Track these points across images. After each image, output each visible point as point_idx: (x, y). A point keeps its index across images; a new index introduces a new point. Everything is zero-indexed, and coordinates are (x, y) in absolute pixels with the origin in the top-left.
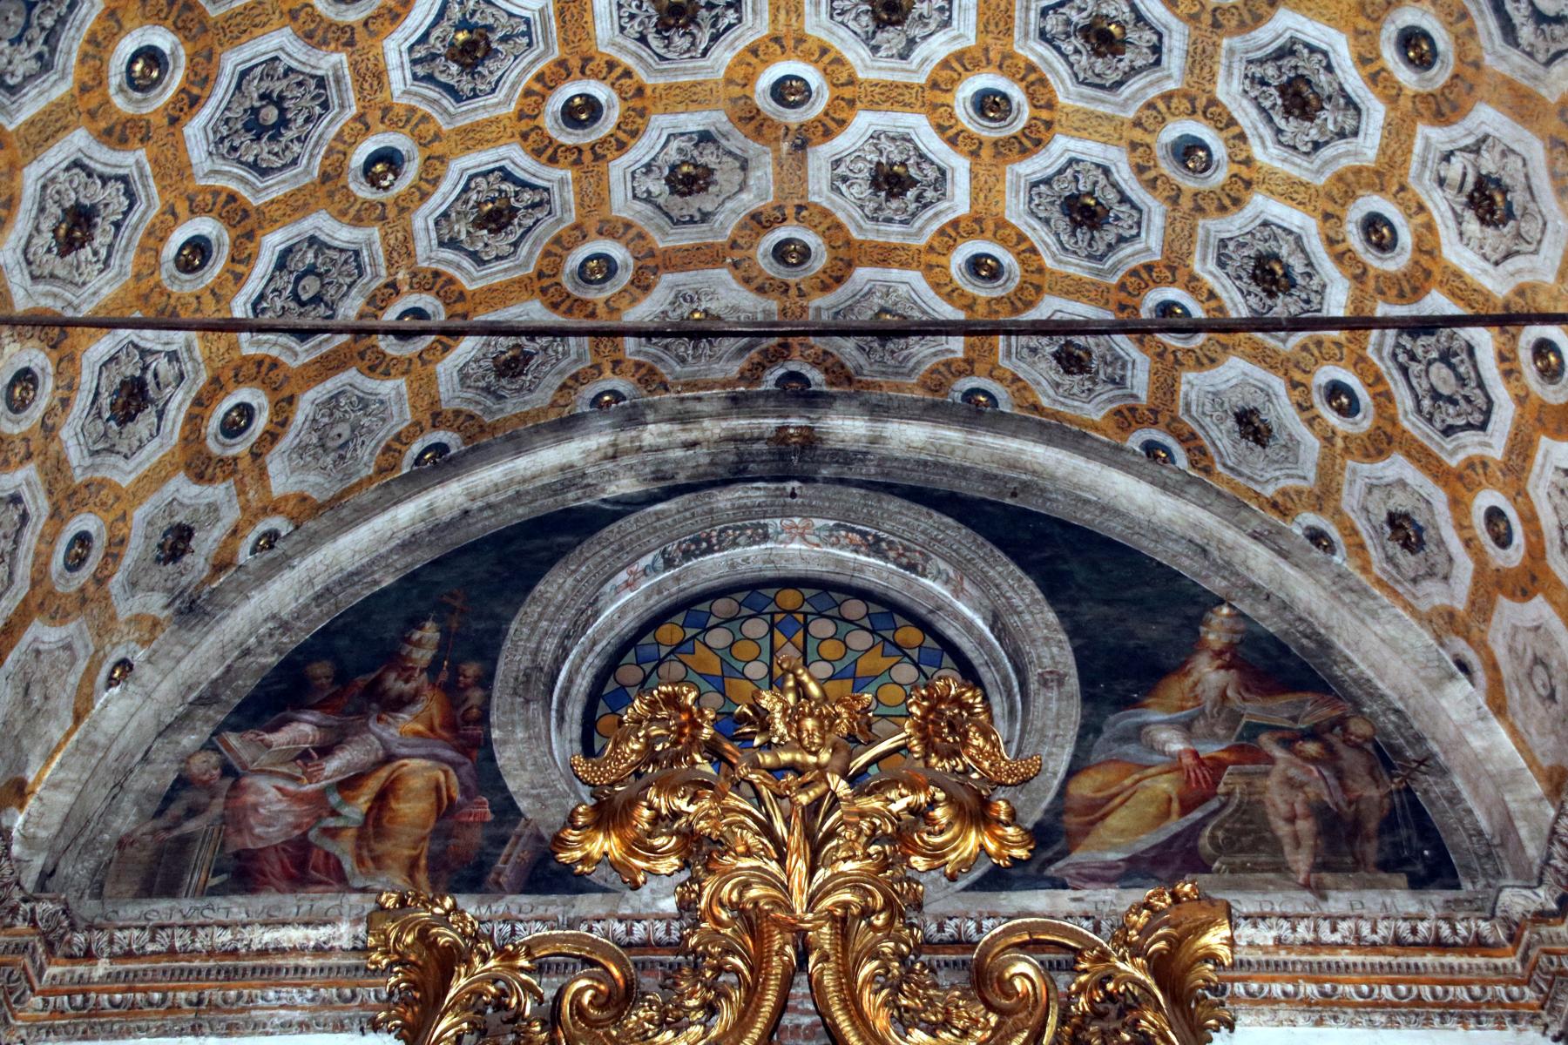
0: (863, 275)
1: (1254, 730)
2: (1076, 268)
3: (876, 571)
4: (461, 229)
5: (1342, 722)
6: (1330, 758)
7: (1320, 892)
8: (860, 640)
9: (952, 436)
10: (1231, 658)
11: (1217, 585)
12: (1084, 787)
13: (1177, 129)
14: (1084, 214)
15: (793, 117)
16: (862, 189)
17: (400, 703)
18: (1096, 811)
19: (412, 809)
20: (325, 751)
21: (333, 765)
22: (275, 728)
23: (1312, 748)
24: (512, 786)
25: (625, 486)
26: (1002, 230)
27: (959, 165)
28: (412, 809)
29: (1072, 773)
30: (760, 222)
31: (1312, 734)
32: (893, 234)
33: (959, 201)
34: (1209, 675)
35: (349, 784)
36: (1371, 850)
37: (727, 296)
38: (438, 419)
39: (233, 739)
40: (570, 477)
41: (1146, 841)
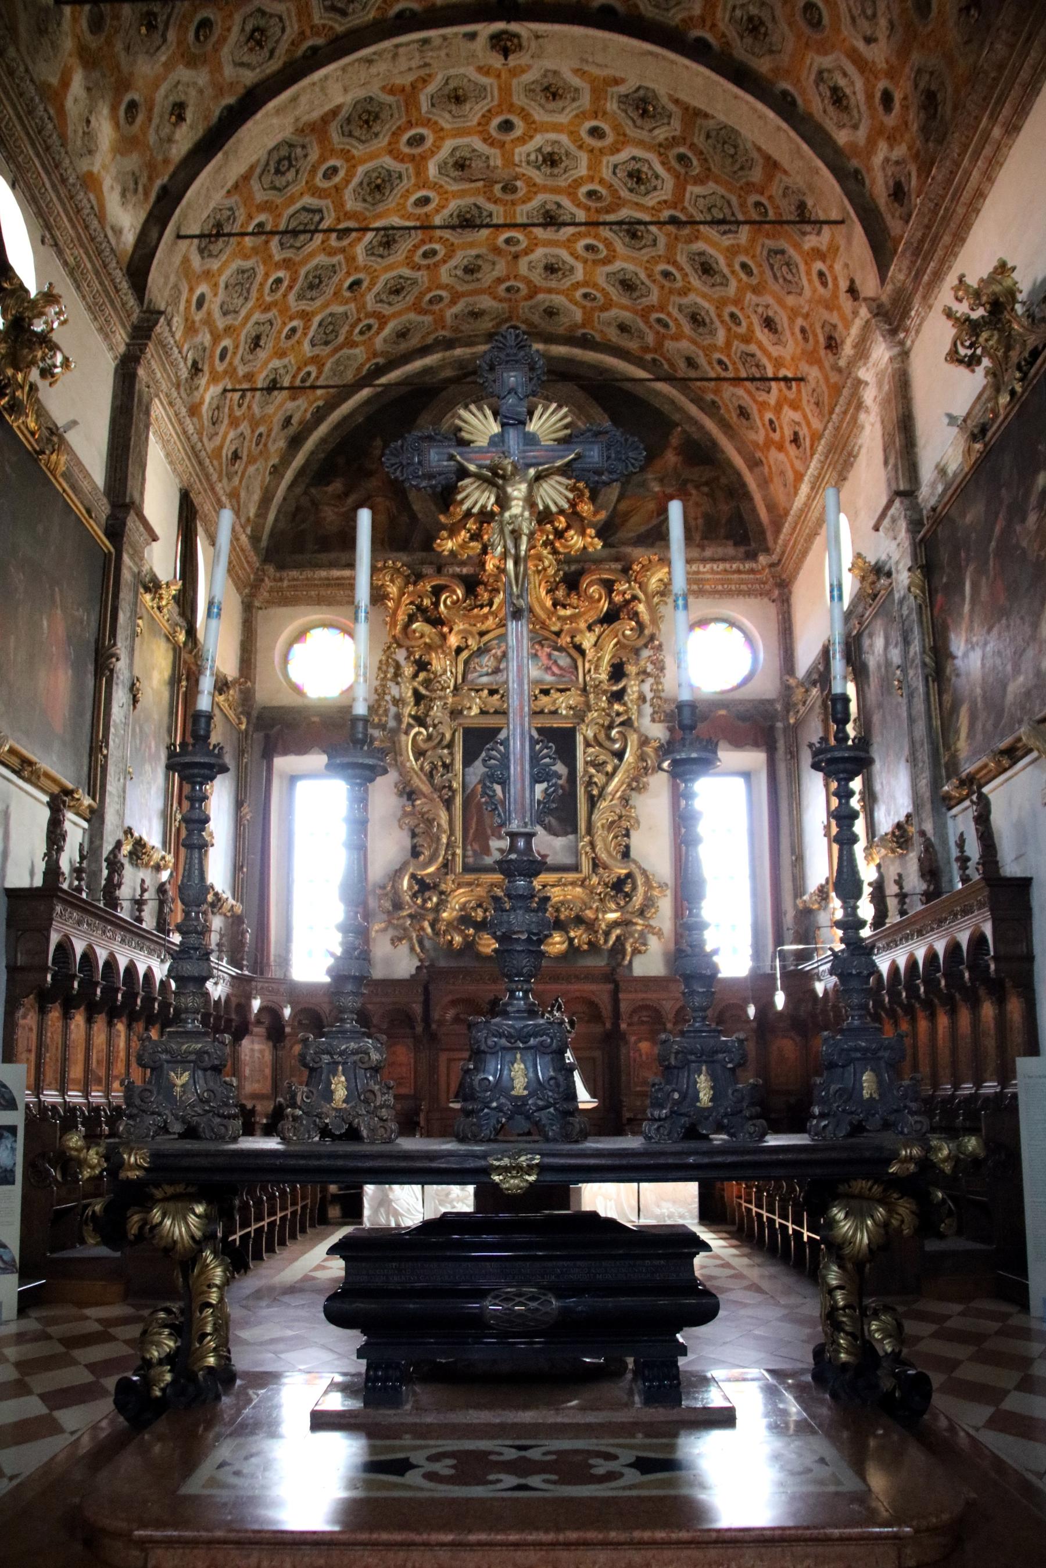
0: (541, 296)
1: (686, 482)
2: (625, 301)
4: (384, 297)
5: (717, 478)
6: (711, 495)
7: (703, 548)
9: (577, 352)
10: (680, 451)
11: (676, 417)
12: (623, 506)
13: (663, 267)
14: (627, 285)
15: (513, 249)
16: (540, 270)
18: (627, 516)
20: (346, 494)
22: (328, 484)
23: (705, 489)
24: (415, 507)
25: (448, 373)
26: (595, 285)
27: (579, 267)
29: (618, 500)
30: (499, 281)
31: (707, 484)
32: (553, 284)
33: (579, 275)
34: (671, 458)
36: (723, 531)
37: (486, 302)
38: (375, 355)
39: (313, 491)
40: (427, 371)
41: (643, 529)
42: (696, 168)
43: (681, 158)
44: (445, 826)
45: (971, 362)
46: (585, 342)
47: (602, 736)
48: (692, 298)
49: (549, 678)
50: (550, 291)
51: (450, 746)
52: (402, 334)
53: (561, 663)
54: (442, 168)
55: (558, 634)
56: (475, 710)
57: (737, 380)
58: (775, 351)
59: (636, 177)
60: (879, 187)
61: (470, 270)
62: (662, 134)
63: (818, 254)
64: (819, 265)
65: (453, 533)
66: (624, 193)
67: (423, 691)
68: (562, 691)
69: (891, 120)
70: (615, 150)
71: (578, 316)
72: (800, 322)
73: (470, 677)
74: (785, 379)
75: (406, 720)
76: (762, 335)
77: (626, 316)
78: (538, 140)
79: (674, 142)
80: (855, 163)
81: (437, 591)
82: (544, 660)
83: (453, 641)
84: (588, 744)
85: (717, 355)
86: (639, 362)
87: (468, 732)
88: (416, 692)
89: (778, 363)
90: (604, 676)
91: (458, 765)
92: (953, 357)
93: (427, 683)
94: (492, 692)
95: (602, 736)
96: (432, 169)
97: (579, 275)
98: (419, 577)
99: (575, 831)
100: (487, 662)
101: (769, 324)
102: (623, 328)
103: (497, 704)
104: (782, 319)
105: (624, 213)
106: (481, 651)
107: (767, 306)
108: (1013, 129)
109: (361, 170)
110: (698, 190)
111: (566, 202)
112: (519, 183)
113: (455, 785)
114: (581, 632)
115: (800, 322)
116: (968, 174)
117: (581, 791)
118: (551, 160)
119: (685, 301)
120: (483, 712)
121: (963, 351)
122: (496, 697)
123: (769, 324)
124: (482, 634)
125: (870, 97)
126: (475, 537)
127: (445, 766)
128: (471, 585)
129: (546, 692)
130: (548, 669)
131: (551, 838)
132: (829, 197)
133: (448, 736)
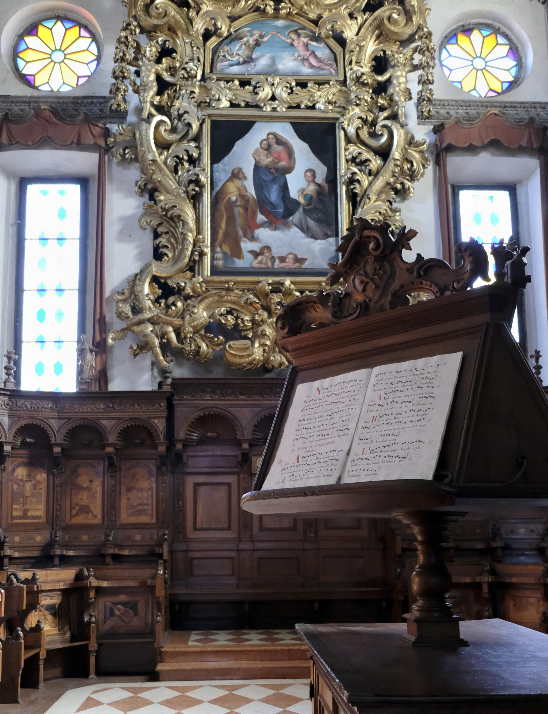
44: (192, 224)
47: (364, 134)
49: (306, 70)
51: (197, 139)
53: (319, 54)
55: (315, 22)
56: (225, 103)
67: (167, 77)
68: (320, 83)
73: (219, 66)
75: (148, 108)
84: (348, 141)
87: (215, 125)
88: (159, 78)
90: (366, 69)
91: (206, 159)
93: (172, 70)
94: (244, 83)
95: (364, 134)
100: (238, 50)
103: (249, 98)
106: (231, 38)
113: (203, 179)
114: (343, 18)
117: (342, 191)
120: (233, 105)
122: (249, 88)
124: (233, 19)
127: (192, 161)
129: (303, 85)
133: (195, 126)
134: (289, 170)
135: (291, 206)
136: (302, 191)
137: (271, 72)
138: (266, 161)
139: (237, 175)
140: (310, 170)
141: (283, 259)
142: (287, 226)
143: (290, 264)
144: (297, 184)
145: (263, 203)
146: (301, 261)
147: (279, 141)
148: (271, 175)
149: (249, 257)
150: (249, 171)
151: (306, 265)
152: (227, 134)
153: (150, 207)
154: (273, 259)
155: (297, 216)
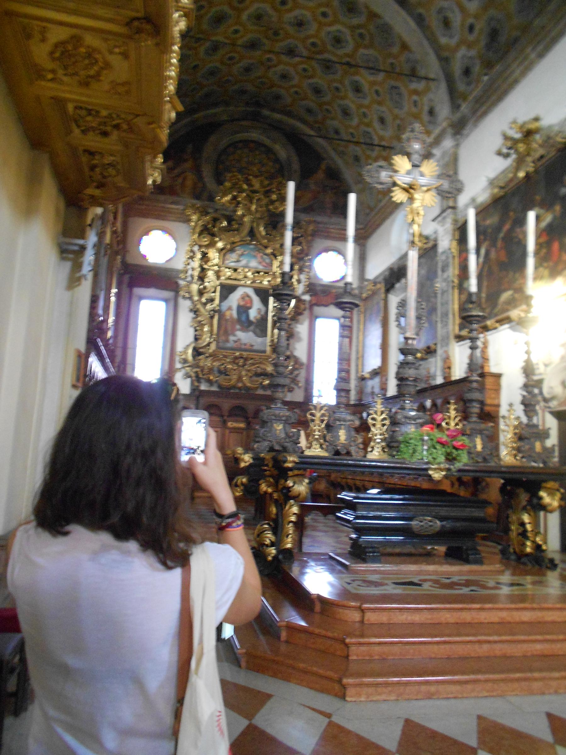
0: (274, 89)
3: (267, 142)
8: (264, 156)
9: (285, 118)
11: (325, 156)
15: (269, 63)
17: (186, 161)
19: (189, 183)
21: (176, 171)
25: (225, 117)
28: (189, 183)
33: (296, 81)
35: (178, 176)
37: (250, 87)
42: (367, 42)
43: (361, 36)
45: (506, 156)
46: (289, 114)
48: (346, 102)
49: (260, 267)
50: (280, 87)
51: (214, 292)
52: (207, 95)
54: (249, 17)
57: (357, 143)
58: (381, 133)
59: (338, 41)
60: (457, 68)
61: (248, 70)
62: (355, 21)
63: (416, 92)
64: (415, 97)
65: (225, 195)
66: (329, 47)
69: (471, 38)
70: (330, 25)
71: (289, 100)
72: (398, 122)
74: (384, 147)
76: (376, 125)
77: (312, 105)
78: (297, 12)
79: (359, 26)
80: (446, 54)
81: (215, 220)
82: (259, 259)
83: (220, 245)
85: (351, 130)
86: (312, 128)
87: (222, 286)
89: (382, 138)
92: (499, 153)
96: (244, 17)
97: (296, 81)
98: (207, 213)
99: (265, 335)
100: (233, 257)
101: (382, 120)
102: (309, 111)
104: (389, 119)
105: (326, 56)
107: (383, 112)
108: (541, 56)
109: (214, 10)
110: (366, 52)
111: (300, 46)
112: (281, 32)
115: (398, 122)
116: (513, 72)
118: (300, 24)
119: (342, 102)
121: (505, 151)
123: (382, 120)
125: (462, 25)
126: (234, 198)
128: (230, 220)
129: (258, 272)
130: (260, 263)
131: (257, 338)
132: (433, 67)
134: (250, 308)
135: (250, 323)
136: (255, 317)
137: (246, 266)
138: (242, 303)
139: (230, 308)
140: (259, 309)
141: (245, 344)
142: (249, 331)
143: (247, 347)
144: (253, 314)
145: (239, 321)
146: (252, 346)
147: (248, 296)
148: (243, 309)
149: (232, 342)
150: (235, 307)
151: (255, 348)
152: (227, 290)
153: (194, 318)
154: (241, 344)
155: (252, 328)
